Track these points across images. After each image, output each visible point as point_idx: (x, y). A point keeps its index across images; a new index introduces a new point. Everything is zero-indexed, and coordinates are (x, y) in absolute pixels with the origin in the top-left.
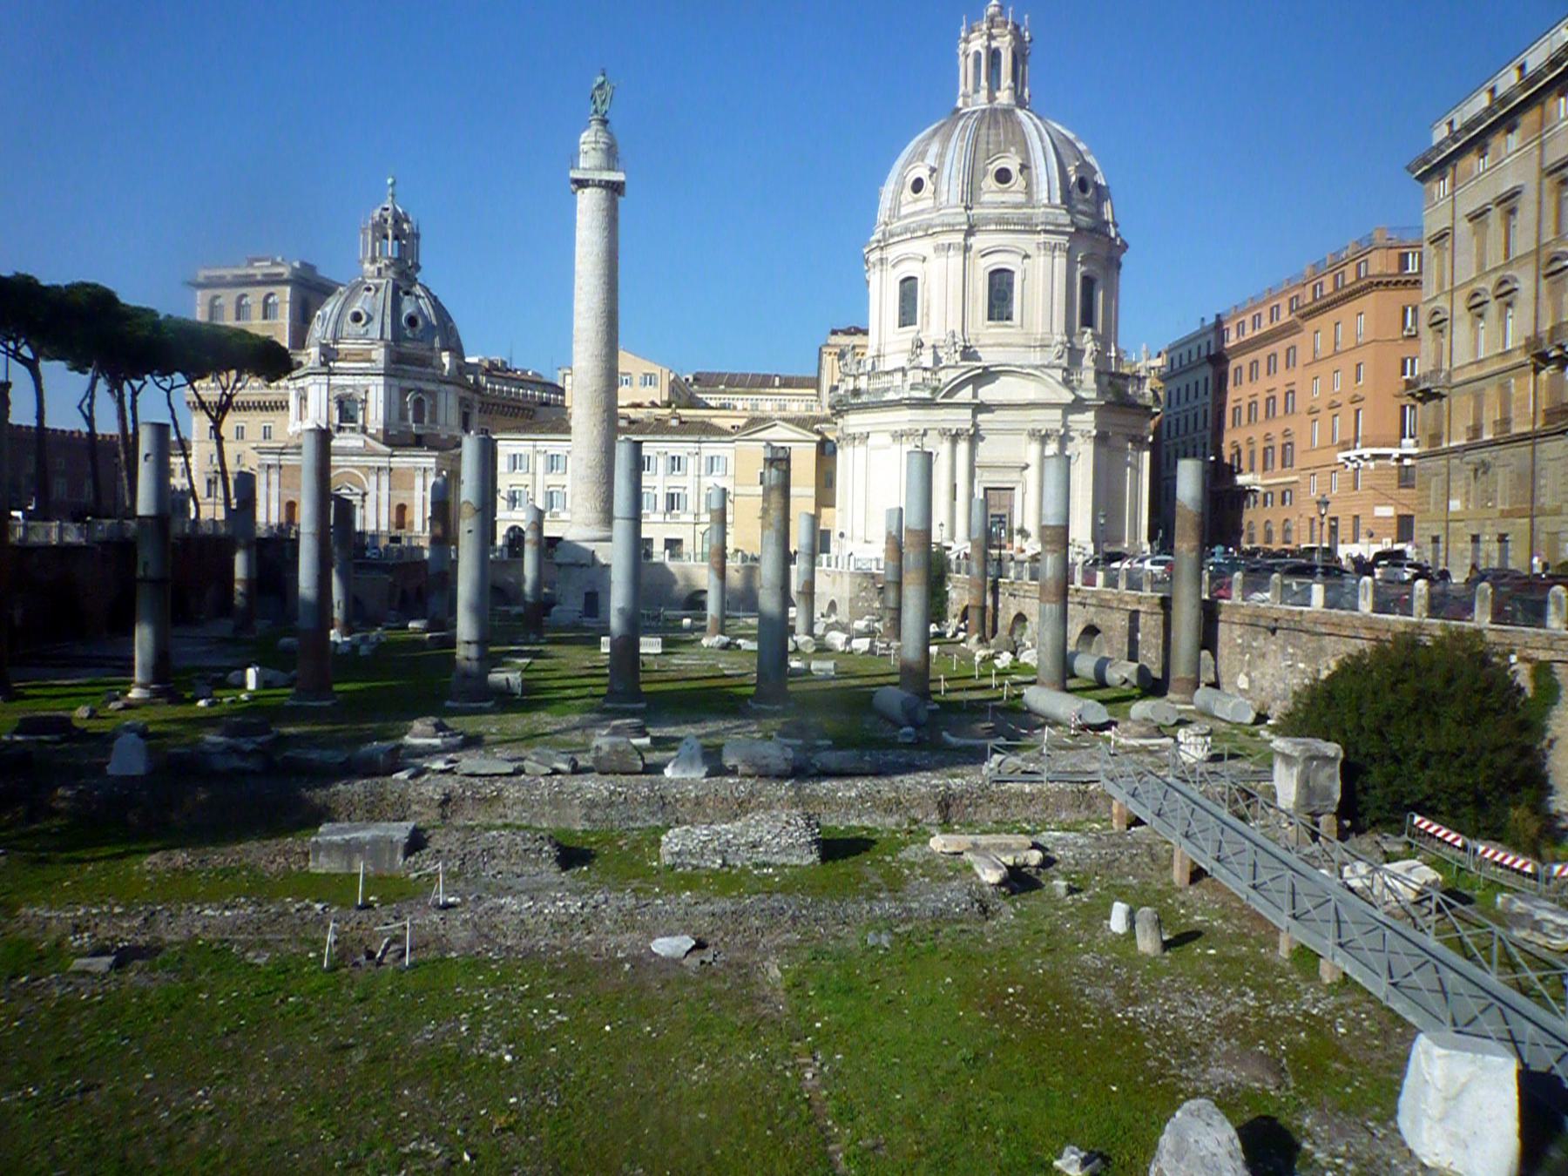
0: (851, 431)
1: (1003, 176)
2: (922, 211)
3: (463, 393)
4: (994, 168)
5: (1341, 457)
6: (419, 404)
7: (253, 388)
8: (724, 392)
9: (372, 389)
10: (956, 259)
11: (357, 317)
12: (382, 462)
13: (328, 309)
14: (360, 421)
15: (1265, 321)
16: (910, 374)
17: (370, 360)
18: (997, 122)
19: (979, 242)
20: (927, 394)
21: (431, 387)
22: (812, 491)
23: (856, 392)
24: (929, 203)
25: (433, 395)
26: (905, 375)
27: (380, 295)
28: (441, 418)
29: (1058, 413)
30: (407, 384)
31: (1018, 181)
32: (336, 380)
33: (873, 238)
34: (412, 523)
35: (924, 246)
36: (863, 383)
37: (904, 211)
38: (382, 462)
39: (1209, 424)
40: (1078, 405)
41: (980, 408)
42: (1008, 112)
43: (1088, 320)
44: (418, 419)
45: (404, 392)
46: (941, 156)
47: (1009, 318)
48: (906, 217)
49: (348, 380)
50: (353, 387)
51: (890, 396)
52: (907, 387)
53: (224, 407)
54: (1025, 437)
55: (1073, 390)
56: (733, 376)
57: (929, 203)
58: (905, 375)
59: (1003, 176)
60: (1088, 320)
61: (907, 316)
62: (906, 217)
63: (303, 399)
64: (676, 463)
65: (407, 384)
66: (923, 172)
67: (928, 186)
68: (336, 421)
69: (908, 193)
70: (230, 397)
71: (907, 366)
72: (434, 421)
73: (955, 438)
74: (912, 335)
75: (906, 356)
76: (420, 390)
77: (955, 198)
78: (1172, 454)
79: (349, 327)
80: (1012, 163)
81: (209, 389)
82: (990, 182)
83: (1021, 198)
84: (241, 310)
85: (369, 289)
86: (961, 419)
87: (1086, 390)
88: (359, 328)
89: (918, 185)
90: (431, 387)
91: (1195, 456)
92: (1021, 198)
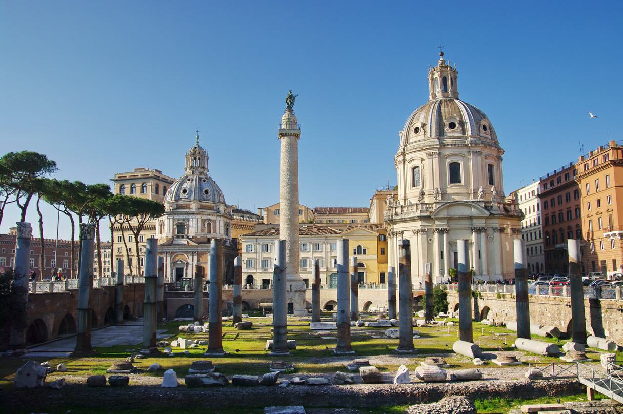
0: (395, 231)
2: (420, 141)
3: (225, 219)
4: (447, 123)
5: (605, 234)
6: (209, 225)
7: (149, 221)
8: (328, 216)
9: (191, 219)
11: (185, 191)
13: (173, 188)
14: (186, 233)
15: (563, 179)
16: (420, 206)
17: (189, 208)
18: (447, 104)
19: (446, 152)
20: (428, 214)
21: (214, 218)
22: (376, 257)
23: (397, 214)
24: (422, 137)
25: (215, 221)
26: (417, 207)
27: (194, 182)
28: (218, 232)
29: (483, 221)
30: (205, 217)
32: (176, 217)
33: (399, 152)
34: (206, 275)
35: (422, 155)
36: (399, 211)
37: (411, 140)
39: (541, 223)
41: (449, 219)
43: (491, 182)
44: (209, 232)
45: (203, 221)
46: (426, 118)
47: (460, 182)
48: (413, 143)
49: (181, 217)
50: (183, 219)
51: (412, 215)
52: (419, 211)
53: (141, 227)
54: (470, 231)
55: (488, 210)
56: (331, 209)
57: (422, 137)
58: (417, 207)
59: (452, 125)
60: (491, 182)
62: (413, 143)
63: (162, 225)
64: (318, 247)
66: (419, 125)
67: (421, 131)
68: (176, 233)
69: (412, 133)
70: (142, 225)
71: (418, 203)
72: (215, 232)
73: (441, 232)
74: (419, 190)
75: (418, 198)
76: (209, 220)
77: (434, 134)
78: (566, 235)
79: (182, 196)
81: (135, 221)
83: (460, 135)
84: (132, 189)
85: (189, 180)
87: (493, 211)
88: (185, 196)
89: (417, 130)
90: (214, 218)
91: (572, 238)
92: (460, 135)
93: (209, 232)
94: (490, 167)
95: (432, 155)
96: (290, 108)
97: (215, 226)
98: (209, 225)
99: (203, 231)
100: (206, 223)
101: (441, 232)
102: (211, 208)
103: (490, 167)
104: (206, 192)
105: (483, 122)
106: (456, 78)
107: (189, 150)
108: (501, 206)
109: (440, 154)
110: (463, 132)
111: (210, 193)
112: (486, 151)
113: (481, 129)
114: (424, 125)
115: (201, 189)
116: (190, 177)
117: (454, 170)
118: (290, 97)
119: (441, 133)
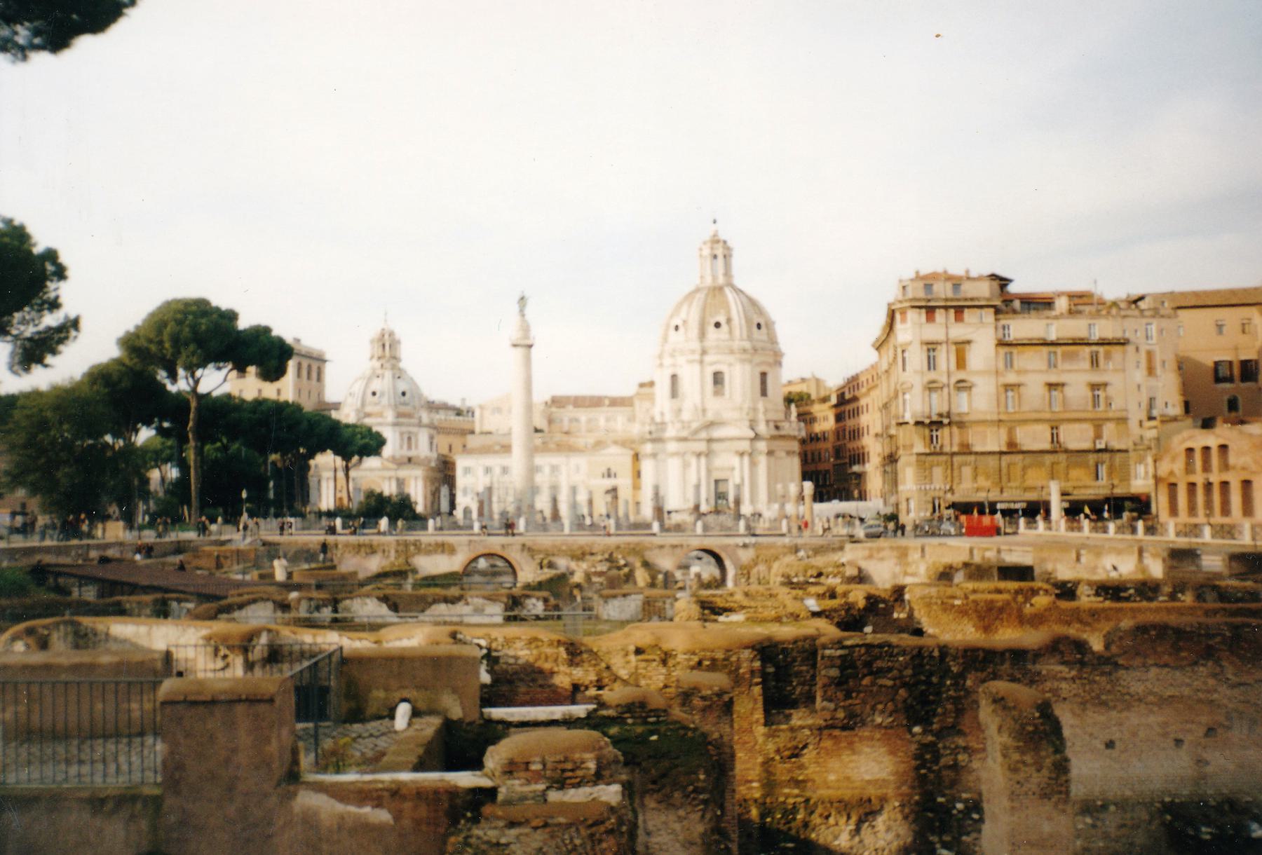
1: (718, 325)
4: (713, 321)
6: (409, 439)
10: (697, 367)
12: (392, 473)
19: (708, 359)
25: (416, 435)
31: (724, 327)
38: (392, 473)
40: (757, 437)
41: (710, 441)
42: (721, 289)
44: (409, 447)
45: (402, 434)
46: (688, 313)
59: (718, 325)
61: (674, 393)
65: (404, 429)
66: (679, 322)
67: (681, 329)
72: (417, 447)
73: (699, 455)
80: (722, 319)
82: (711, 328)
86: (702, 447)
89: (677, 328)
92: (727, 336)
93: (409, 447)
94: (764, 375)
95: (691, 362)
96: (522, 313)
97: (417, 441)
98: (409, 439)
99: (401, 447)
100: (406, 437)
101: (699, 455)
102: (409, 416)
103: (764, 375)
104: (404, 394)
105: (757, 319)
106: (731, 256)
107: (374, 332)
108: (772, 425)
109: (701, 362)
110: (730, 332)
111: (408, 395)
112: (758, 359)
113: (755, 328)
114: (685, 322)
115: (395, 387)
116: (379, 372)
117: (718, 378)
118: (522, 298)
119: (702, 335)
